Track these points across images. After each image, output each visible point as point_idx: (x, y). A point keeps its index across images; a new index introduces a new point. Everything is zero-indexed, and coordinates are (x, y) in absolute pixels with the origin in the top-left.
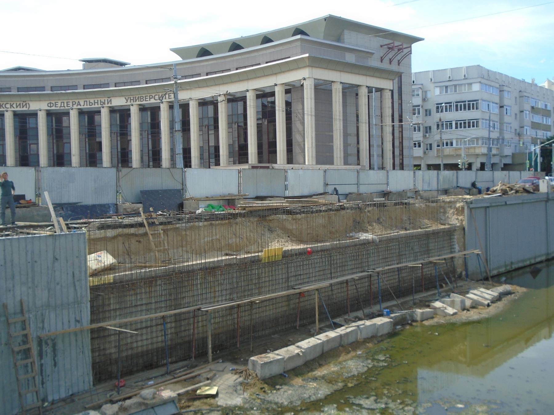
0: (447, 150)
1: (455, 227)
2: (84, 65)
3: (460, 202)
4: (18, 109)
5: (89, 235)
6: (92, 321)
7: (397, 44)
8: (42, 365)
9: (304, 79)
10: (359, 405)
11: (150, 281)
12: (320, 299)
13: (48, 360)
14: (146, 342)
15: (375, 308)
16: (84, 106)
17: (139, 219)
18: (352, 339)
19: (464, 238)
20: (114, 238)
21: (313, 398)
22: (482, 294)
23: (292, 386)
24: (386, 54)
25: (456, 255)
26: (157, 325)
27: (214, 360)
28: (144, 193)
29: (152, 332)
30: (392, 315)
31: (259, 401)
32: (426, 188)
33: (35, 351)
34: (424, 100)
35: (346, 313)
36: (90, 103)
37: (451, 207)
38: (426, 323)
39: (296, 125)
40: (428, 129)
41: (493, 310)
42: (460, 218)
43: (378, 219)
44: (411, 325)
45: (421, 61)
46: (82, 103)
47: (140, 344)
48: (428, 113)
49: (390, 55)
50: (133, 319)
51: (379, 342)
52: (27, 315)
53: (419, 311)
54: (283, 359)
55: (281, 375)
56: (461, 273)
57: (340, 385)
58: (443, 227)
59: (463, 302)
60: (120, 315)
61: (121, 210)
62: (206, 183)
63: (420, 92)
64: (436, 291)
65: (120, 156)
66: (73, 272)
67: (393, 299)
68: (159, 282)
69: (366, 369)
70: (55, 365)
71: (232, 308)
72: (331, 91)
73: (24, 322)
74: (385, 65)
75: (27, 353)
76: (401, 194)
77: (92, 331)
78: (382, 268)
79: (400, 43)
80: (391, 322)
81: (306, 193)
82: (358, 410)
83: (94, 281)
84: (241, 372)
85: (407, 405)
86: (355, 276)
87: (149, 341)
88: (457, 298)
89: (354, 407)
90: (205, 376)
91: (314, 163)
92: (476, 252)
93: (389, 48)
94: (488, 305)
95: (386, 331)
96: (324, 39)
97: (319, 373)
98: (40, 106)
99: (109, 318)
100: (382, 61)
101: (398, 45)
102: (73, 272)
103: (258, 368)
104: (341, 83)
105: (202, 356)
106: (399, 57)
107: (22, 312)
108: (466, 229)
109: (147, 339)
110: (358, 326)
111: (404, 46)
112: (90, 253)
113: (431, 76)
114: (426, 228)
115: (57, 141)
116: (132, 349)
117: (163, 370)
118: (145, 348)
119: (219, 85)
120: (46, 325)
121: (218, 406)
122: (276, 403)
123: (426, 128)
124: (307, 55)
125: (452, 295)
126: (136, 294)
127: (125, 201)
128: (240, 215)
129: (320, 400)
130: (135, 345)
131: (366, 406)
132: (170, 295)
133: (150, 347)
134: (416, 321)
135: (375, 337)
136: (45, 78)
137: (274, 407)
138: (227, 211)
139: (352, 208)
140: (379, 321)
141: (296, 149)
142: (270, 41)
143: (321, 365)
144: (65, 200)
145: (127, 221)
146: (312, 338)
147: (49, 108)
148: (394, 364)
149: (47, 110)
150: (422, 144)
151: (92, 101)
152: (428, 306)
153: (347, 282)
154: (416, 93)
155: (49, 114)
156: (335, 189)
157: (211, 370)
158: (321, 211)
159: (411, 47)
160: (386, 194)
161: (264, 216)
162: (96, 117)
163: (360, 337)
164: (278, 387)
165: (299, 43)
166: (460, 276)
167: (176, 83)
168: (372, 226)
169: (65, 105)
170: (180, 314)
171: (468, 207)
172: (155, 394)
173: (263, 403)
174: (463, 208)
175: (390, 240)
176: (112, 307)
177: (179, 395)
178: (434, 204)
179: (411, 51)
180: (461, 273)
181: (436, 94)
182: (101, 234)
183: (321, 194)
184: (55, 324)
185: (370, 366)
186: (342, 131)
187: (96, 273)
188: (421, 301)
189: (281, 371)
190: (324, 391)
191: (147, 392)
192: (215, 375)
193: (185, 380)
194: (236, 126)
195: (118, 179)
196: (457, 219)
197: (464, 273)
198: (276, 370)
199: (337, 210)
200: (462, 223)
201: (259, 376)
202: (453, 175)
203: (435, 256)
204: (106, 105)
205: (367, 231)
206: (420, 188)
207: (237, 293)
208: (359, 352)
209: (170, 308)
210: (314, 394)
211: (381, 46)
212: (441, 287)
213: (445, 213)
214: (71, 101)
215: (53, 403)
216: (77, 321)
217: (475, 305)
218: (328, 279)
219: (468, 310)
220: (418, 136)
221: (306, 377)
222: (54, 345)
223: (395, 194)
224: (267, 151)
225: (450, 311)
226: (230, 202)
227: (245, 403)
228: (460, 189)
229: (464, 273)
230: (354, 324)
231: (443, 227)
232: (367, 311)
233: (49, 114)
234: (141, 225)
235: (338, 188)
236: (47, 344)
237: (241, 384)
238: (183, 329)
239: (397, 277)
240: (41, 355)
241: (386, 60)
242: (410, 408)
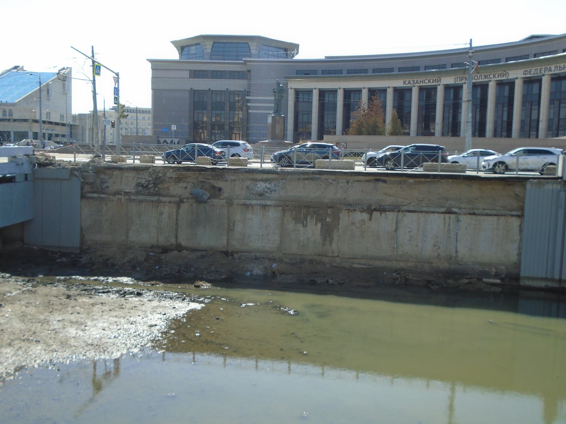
36: (560, 68)
46: (553, 69)
98: (517, 75)
151: (562, 65)
169: (538, 72)
214: (543, 67)
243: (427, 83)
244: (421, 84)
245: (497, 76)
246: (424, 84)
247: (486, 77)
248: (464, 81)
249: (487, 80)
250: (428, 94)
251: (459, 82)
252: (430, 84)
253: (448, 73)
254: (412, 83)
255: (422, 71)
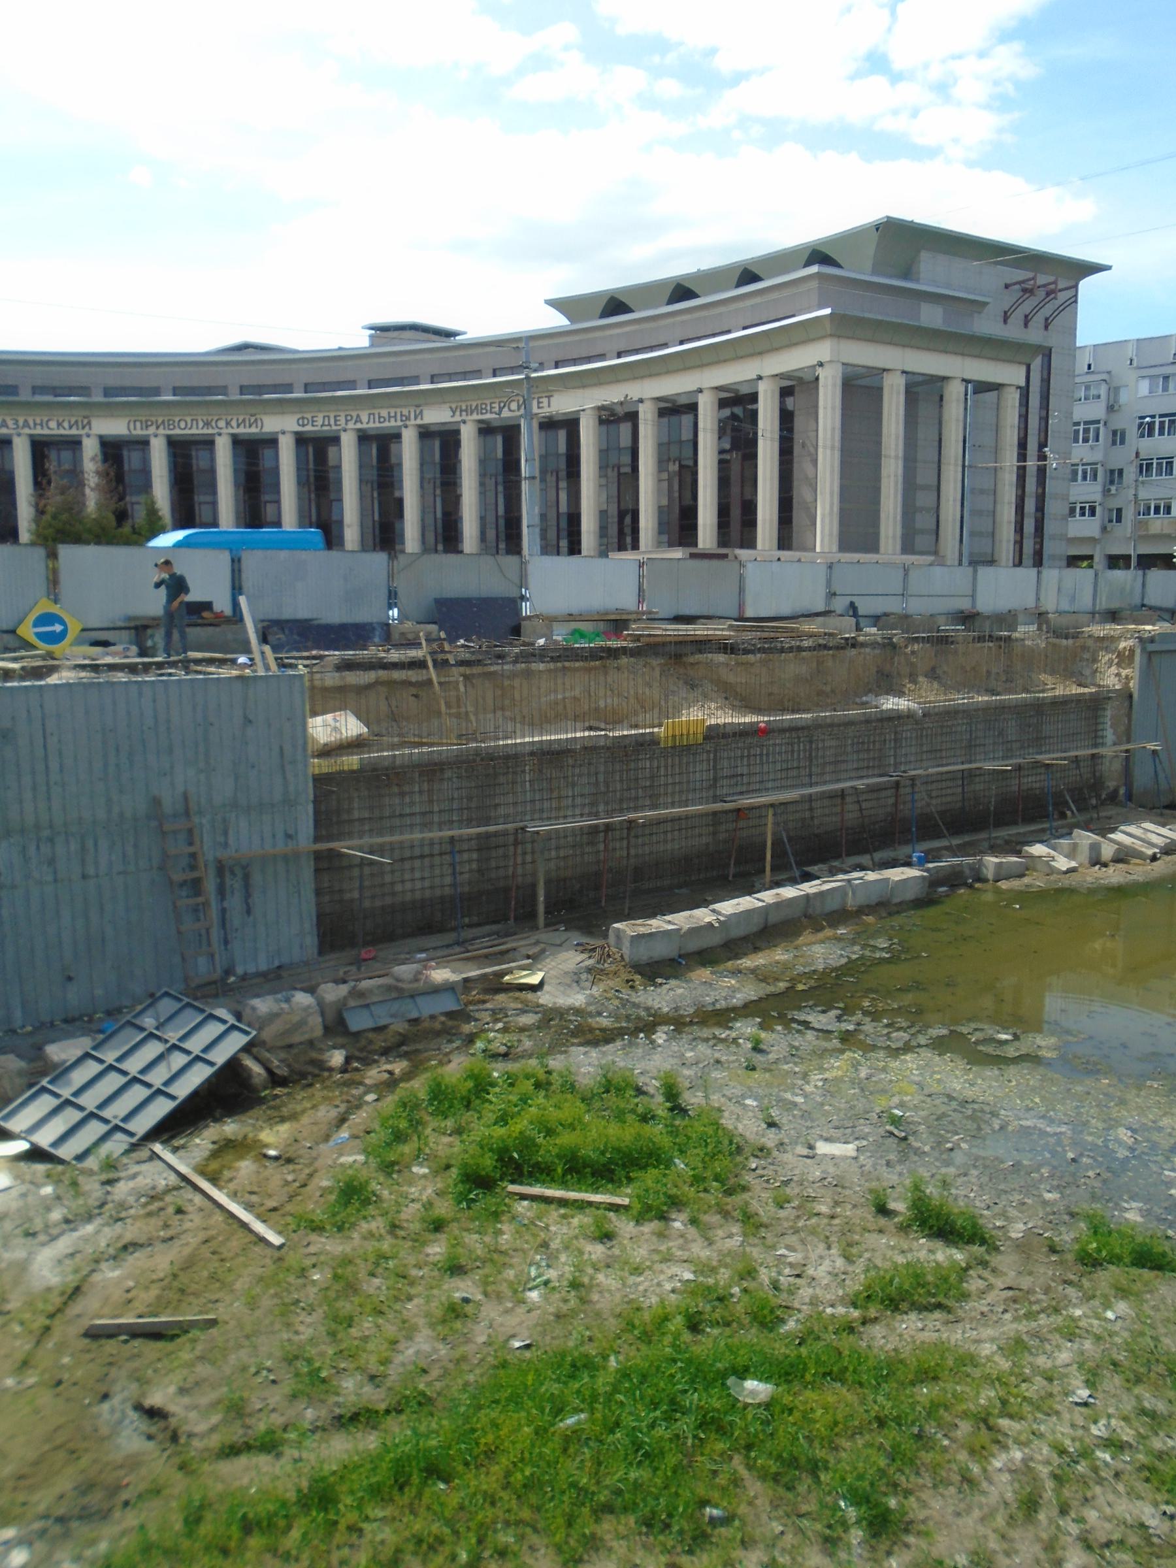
0: (1157, 524)
1: (1109, 691)
2: (371, 336)
3: (1126, 639)
4: (241, 430)
5: (311, 680)
6: (317, 839)
7: (1042, 279)
8: (224, 911)
9: (821, 364)
10: (806, 1024)
11: (432, 770)
12: (776, 824)
13: (235, 902)
14: (420, 883)
15: (902, 851)
16: (369, 421)
17: (414, 653)
18: (833, 905)
19: (1129, 716)
20: (369, 687)
21: (722, 1004)
22: (1145, 834)
23: (687, 981)
24: (1016, 305)
25: (1107, 751)
26: (441, 854)
27: (547, 925)
28: (441, 603)
29: (432, 866)
30: (931, 865)
31: (616, 1002)
32: (1065, 606)
33: (210, 885)
34: (1111, 408)
35: (838, 856)
37: (1107, 649)
38: (1004, 885)
39: (801, 466)
40: (1115, 476)
41: (1160, 868)
42: (1124, 673)
43: (933, 669)
44: (971, 886)
45: (1100, 319)
46: (365, 418)
47: (408, 886)
48: (1118, 437)
49: (1027, 307)
50: (396, 838)
51: (890, 914)
52: (196, 820)
53: (992, 860)
54: (679, 930)
55: (672, 960)
56: (1116, 791)
57: (782, 985)
58: (1076, 690)
59: (1095, 848)
60: (371, 830)
61: (396, 636)
62: (564, 588)
63: (1103, 390)
64: (1046, 825)
65: (440, 530)
66: (281, 748)
67: (939, 836)
68: (448, 774)
69: (844, 961)
70: (249, 912)
71: (594, 830)
72: (881, 389)
73: (190, 831)
74: (1013, 331)
75: (196, 886)
76: (1008, 619)
77: (318, 856)
78: (928, 772)
79: (1051, 279)
80: (923, 877)
81: (786, 610)
82: (798, 1031)
83: (319, 766)
84: (594, 950)
85: (899, 1029)
86: (860, 784)
87: (427, 884)
88: (1085, 838)
89: (794, 1025)
90: (524, 951)
91: (835, 548)
92: (1151, 746)
93: (1025, 290)
94: (1154, 858)
95: (910, 895)
96: (875, 272)
97: (747, 962)
98: (282, 425)
99: (350, 835)
100: (1005, 322)
101: (1047, 281)
102: (281, 748)
103: (626, 944)
104: (903, 372)
105: (526, 918)
106: (1047, 311)
107: (187, 813)
108: (1136, 696)
109: (423, 879)
110: (849, 881)
111: (1060, 286)
112: (314, 714)
113: (1130, 352)
114: (1043, 691)
115: (318, 496)
116: (394, 894)
117: (450, 937)
118: (418, 895)
119: (642, 377)
120: (231, 841)
121: (538, 1006)
122: (647, 1009)
123: (1112, 472)
124: (828, 311)
125: (1077, 832)
126: (402, 794)
127: (403, 617)
128: (624, 650)
129: (734, 1009)
130: (399, 888)
131: (817, 1026)
132: (470, 799)
133: (428, 894)
134: (985, 880)
135: (884, 906)
136: (294, 366)
137: (643, 1013)
138: (615, 644)
139: (874, 645)
140: (897, 874)
141: (798, 516)
142: (755, 278)
143: (756, 949)
144: (287, 614)
145: (395, 656)
146: (748, 898)
147: (300, 429)
148: (903, 957)
149: (296, 433)
150: (1098, 510)
151: (384, 413)
152: (1018, 853)
153: (842, 794)
154: (1093, 392)
155: (301, 440)
156: (852, 604)
157: (537, 943)
158: (800, 649)
159: (1076, 287)
160: (967, 618)
161: (679, 657)
162: (393, 447)
163: (851, 903)
164: (659, 980)
165: (814, 284)
166: (1113, 798)
167: (528, 378)
168: (915, 682)
170: (488, 835)
171: (1143, 650)
172: (419, 973)
173: (624, 1006)
174: (1132, 651)
175: (951, 713)
176: (356, 814)
177: (466, 980)
178: (1070, 641)
179: (1076, 296)
180: (1116, 791)
181: (1140, 396)
182: (332, 679)
183: (818, 614)
184: (248, 838)
185: (854, 957)
186: (900, 479)
187: (327, 752)
188: (1007, 842)
189: (674, 954)
190: (749, 992)
191: (404, 971)
192: (543, 951)
193: (486, 956)
194: (676, 467)
195: (391, 576)
196: (1118, 675)
197: (1122, 791)
198: (661, 950)
199: (839, 648)
200: (1127, 684)
201: (626, 957)
202: (1135, 580)
203: (1049, 752)
204: (413, 422)
205: (901, 694)
206: (1049, 604)
207: (607, 803)
208: (842, 931)
209: (469, 823)
210: (726, 999)
211: (1007, 286)
212: (1063, 816)
213: (1095, 660)
214: (343, 414)
215: (244, 978)
216: (289, 836)
217: (1123, 856)
218: (803, 785)
219: (1105, 865)
220: (1088, 491)
221: (722, 967)
222: (246, 878)
223: (988, 617)
224: (737, 523)
225: (1063, 863)
226: (617, 624)
227: (588, 1004)
228: (1146, 611)
229: (1122, 791)
230: (841, 877)
231: (1086, 690)
232: (878, 856)
233: (301, 440)
234: (420, 664)
235: (858, 602)
236: (232, 873)
237: (589, 970)
238: (493, 864)
239: (960, 790)
240: (221, 892)
241: (1017, 317)
242: (901, 1034)
243: (52, 428)
244: (38, 431)
245: (234, 423)
246: (46, 432)
247: (207, 424)
248: (152, 430)
249: (210, 431)
250: (316, 451)
251: (139, 432)
252: (62, 432)
253: (109, 409)
254: (10, 423)
255: (25, 396)
